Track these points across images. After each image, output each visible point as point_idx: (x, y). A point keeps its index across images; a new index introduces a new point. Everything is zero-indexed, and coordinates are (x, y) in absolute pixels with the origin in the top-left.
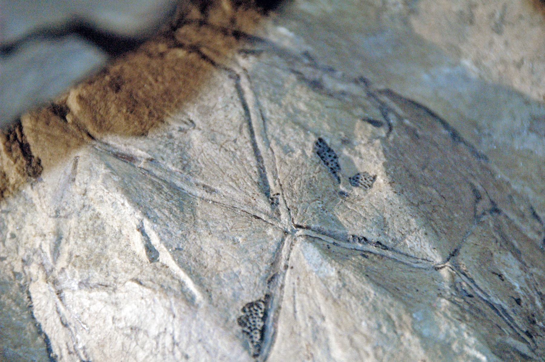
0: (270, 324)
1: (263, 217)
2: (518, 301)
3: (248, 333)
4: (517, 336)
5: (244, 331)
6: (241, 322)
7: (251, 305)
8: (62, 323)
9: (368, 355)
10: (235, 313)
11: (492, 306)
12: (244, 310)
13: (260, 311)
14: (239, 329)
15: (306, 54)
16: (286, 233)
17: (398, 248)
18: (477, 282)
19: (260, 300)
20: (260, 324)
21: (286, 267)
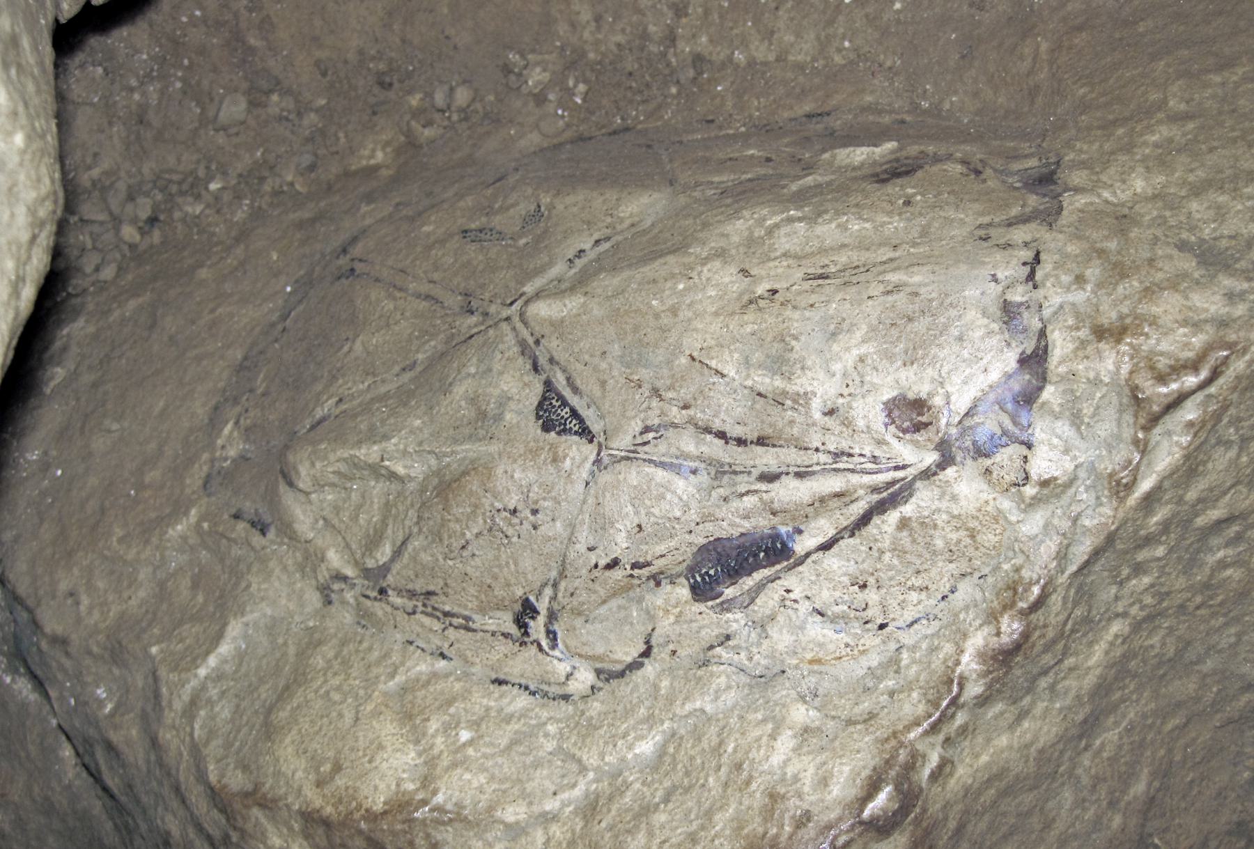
0: (574, 401)
1: (475, 330)
2: (768, 160)
3: (564, 431)
4: (800, 178)
5: (559, 433)
6: (547, 428)
7: (540, 405)
8: (409, 614)
9: (689, 320)
10: (534, 429)
11: (750, 180)
12: (538, 417)
13: (554, 402)
14: (553, 434)
15: (398, 204)
16: (508, 319)
17: (619, 227)
18: (716, 179)
19: (545, 393)
20: (565, 412)
21: (537, 342)
